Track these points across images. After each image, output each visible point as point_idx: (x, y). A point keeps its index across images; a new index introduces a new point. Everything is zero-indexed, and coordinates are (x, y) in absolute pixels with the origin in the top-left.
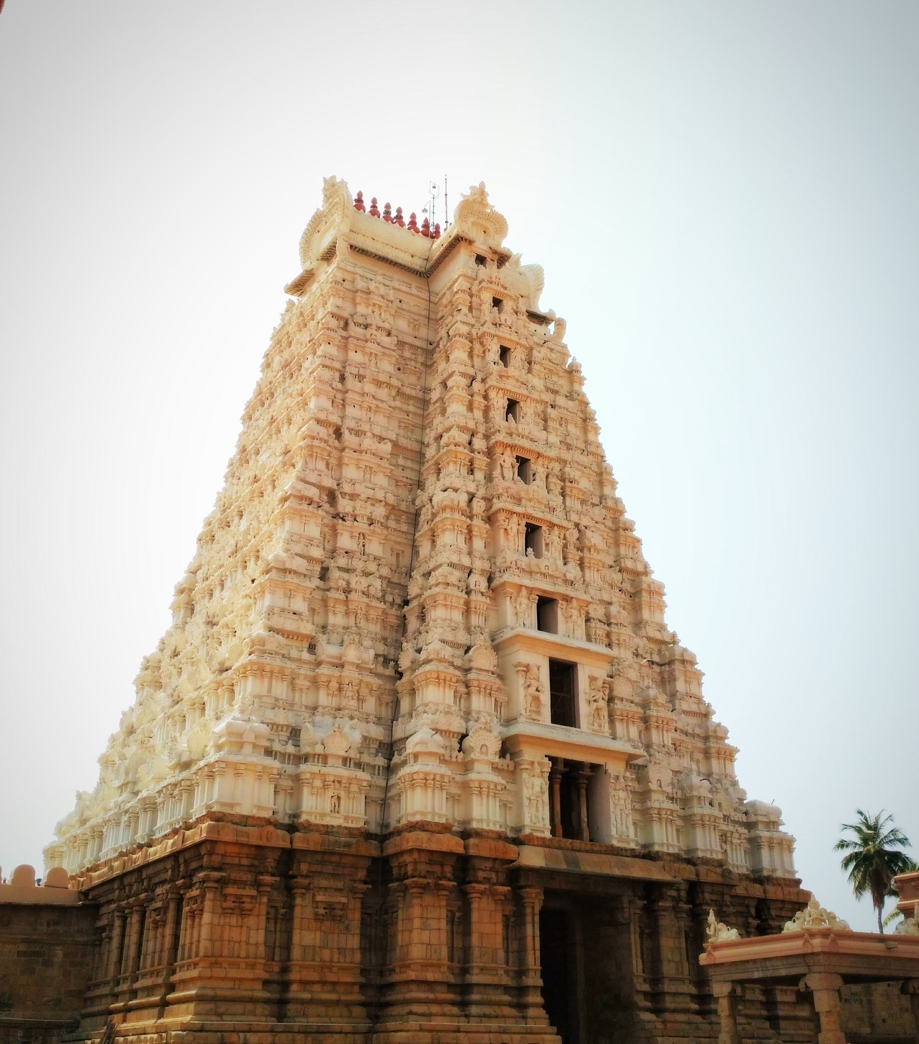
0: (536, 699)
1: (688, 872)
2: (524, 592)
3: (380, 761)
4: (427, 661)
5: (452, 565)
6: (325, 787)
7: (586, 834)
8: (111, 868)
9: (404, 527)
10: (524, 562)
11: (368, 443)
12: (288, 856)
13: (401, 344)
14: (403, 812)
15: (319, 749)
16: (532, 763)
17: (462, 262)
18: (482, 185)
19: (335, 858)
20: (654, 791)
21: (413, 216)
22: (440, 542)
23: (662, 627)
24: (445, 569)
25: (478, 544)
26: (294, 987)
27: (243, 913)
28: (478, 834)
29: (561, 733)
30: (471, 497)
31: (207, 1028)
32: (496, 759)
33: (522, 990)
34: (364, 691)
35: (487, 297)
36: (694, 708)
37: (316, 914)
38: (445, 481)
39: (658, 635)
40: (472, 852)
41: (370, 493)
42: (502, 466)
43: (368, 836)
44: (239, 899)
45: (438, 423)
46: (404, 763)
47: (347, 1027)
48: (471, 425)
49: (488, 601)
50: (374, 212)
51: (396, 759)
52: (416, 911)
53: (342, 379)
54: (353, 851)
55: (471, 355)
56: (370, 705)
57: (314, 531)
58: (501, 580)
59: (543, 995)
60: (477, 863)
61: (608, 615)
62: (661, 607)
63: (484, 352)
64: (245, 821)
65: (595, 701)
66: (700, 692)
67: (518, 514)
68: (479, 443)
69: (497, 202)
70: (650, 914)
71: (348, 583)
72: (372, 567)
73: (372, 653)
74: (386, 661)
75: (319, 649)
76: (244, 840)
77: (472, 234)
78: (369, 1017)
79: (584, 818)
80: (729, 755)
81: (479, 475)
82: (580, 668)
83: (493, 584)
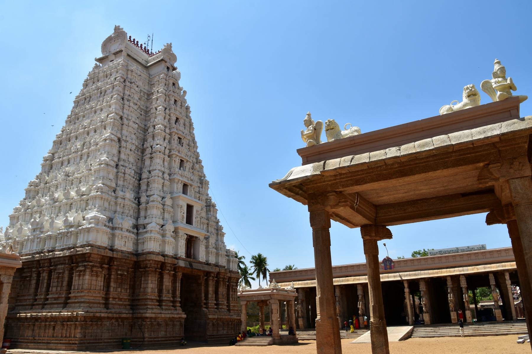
1: (217, 269)
3: (135, 231)
4: (153, 201)
5: (159, 170)
9: (140, 154)
10: (180, 172)
12: (111, 259)
15: (120, 226)
18: (171, 44)
19: (124, 261)
21: (141, 45)
23: (208, 195)
24: (157, 171)
25: (166, 164)
26: (111, 299)
28: (167, 256)
29: (188, 226)
33: (174, 302)
34: (130, 208)
36: (215, 220)
40: (166, 261)
43: (133, 254)
44: (97, 272)
46: (146, 232)
47: (127, 312)
50: (130, 40)
52: (150, 278)
55: (165, 101)
56: (131, 212)
58: (174, 177)
59: (180, 303)
60: (167, 264)
61: (199, 191)
62: (208, 188)
64: (99, 247)
68: (168, 131)
69: (174, 50)
70: (207, 281)
71: (125, 170)
75: (116, 192)
76: (100, 253)
77: (167, 59)
78: (131, 309)
80: (223, 235)
81: (167, 141)
83: (171, 177)
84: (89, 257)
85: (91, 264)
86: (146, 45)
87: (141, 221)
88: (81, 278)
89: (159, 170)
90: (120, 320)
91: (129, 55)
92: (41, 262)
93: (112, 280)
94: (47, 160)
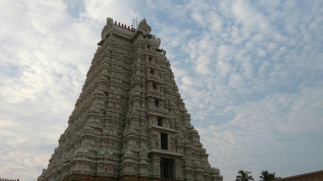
0: (157, 143)
2: (154, 116)
5: (136, 110)
6: (103, 166)
7: (170, 177)
11: (116, 81)
13: (125, 57)
14: (123, 172)
15: (102, 157)
16: (156, 159)
17: (141, 38)
18: (145, 19)
20: (187, 166)
21: (129, 27)
22: (133, 104)
23: (190, 125)
30: (141, 93)
32: (147, 158)
35: (146, 46)
36: (198, 145)
38: (135, 89)
39: (188, 127)
41: (117, 93)
42: (149, 86)
45: (134, 76)
46: (123, 160)
48: (142, 76)
49: (145, 119)
51: (122, 159)
53: (110, 65)
57: (102, 102)
63: (145, 59)
65: (172, 143)
66: (199, 140)
67: (153, 97)
68: (144, 80)
71: (111, 115)
72: (117, 111)
73: (116, 132)
74: (120, 134)
77: (142, 31)
79: (169, 173)
82: (168, 135)
89: (136, 110)
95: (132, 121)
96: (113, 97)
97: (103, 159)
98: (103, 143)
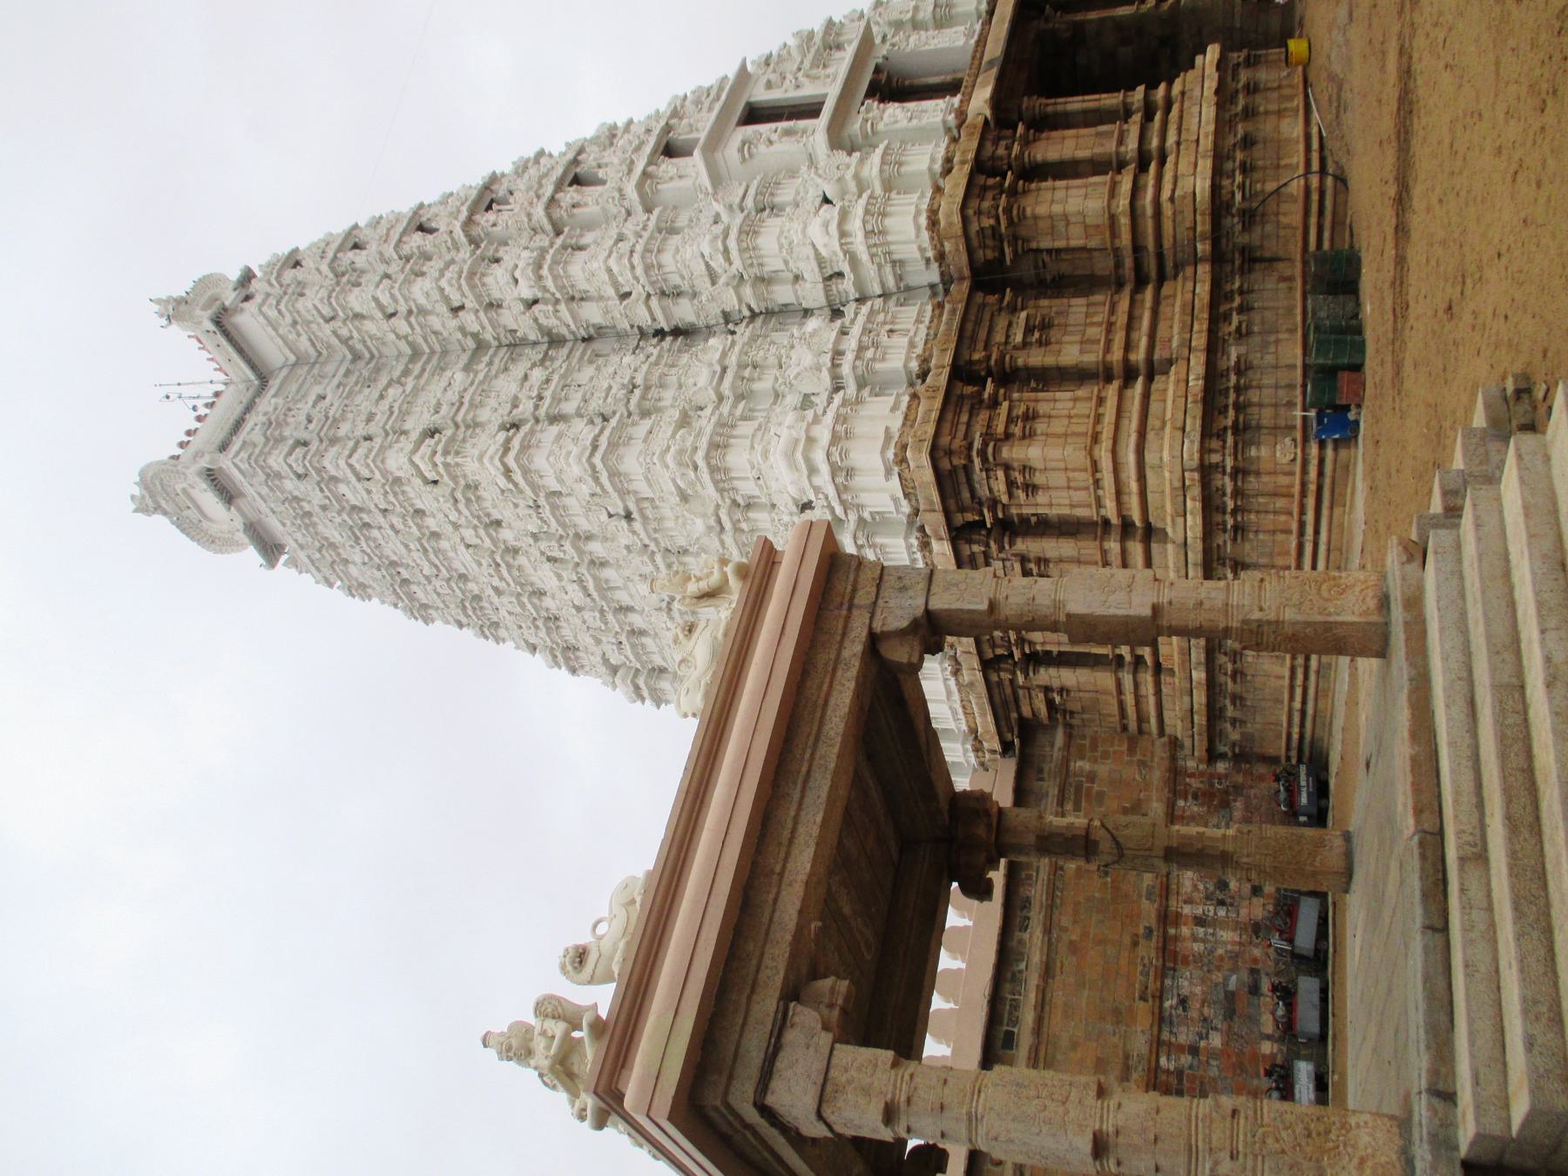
2: (651, 169)
6: (876, 345)
8: (971, 684)
12: (961, 372)
27: (1030, 417)
31: (1180, 424)
35: (289, 275)
37: (1040, 343)
46: (854, 261)
54: (961, 307)
76: (934, 415)
84: (950, 453)
85: (977, 444)
86: (200, 403)
87: (812, 293)
88: (1039, 479)
90: (1223, 308)
91: (224, 447)
92: (989, 654)
93: (1050, 360)
94: (637, 688)
95: (660, 266)
96: (534, 394)
97: (838, 353)
98: (756, 386)
